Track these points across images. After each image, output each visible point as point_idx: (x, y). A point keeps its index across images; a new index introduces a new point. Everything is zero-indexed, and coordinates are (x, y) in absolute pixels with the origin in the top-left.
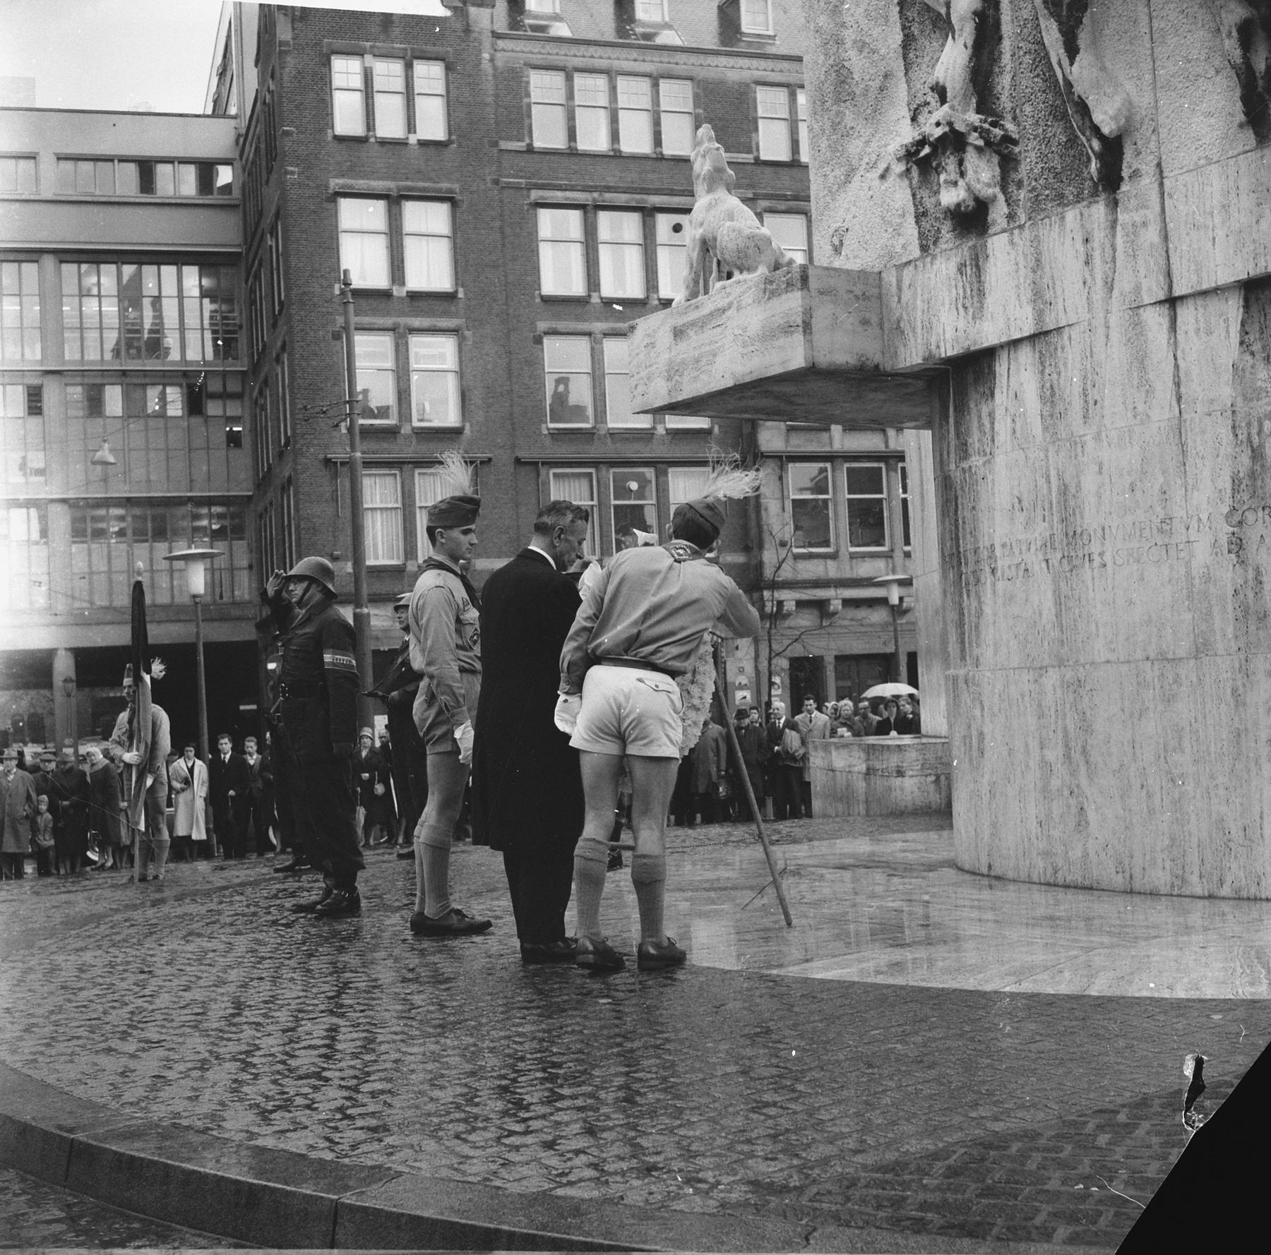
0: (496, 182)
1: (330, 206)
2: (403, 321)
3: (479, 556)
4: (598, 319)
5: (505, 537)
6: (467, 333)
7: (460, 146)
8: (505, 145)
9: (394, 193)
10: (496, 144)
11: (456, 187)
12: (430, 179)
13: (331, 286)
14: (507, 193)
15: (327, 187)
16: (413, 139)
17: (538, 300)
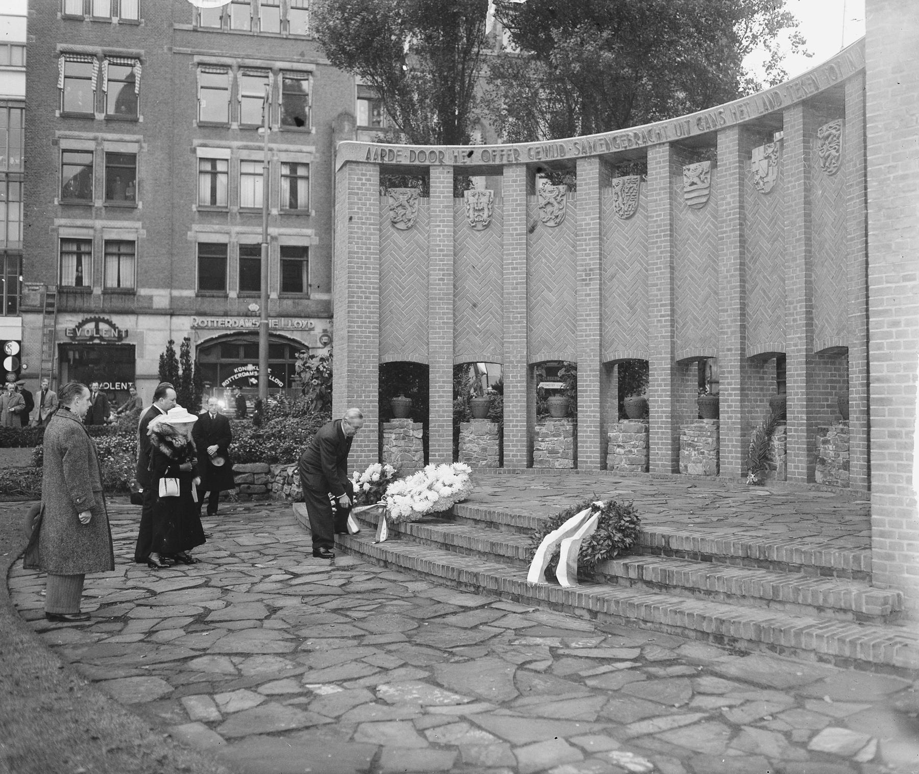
0: (170, 49)
1: (55, 60)
2: (100, 135)
3: (143, 286)
4: (235, 139)
5: (161, 276)
6: (145, 145)
7: (146, 25)
8: (177, 26)
9: (100, 54)
10: (172, 25)
11: (142, 52)
12: (124, 46)
13: (54, 111)
14: (177, 56)
15: (55, 49)
16: (115, 20)
17: (195, 125)
